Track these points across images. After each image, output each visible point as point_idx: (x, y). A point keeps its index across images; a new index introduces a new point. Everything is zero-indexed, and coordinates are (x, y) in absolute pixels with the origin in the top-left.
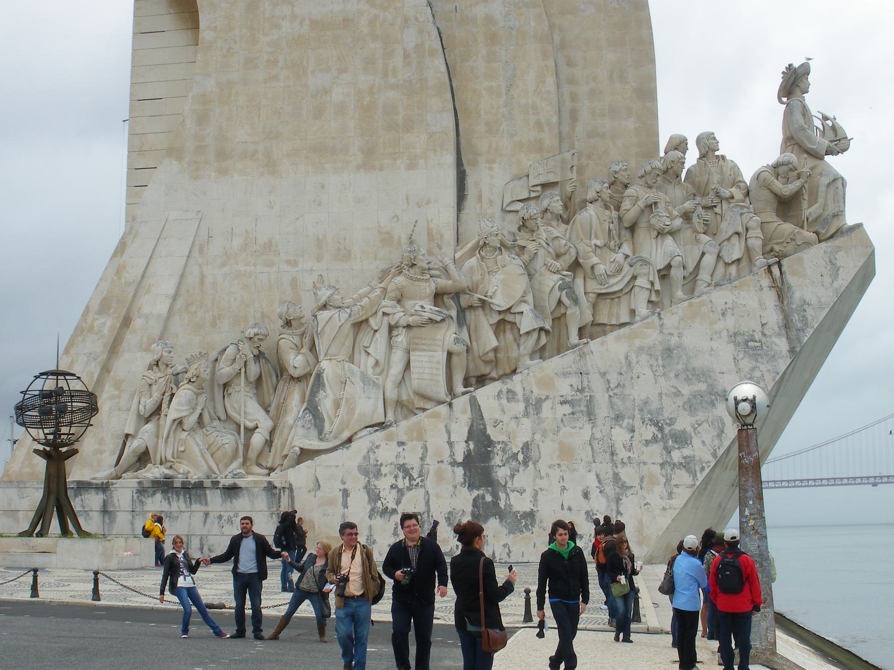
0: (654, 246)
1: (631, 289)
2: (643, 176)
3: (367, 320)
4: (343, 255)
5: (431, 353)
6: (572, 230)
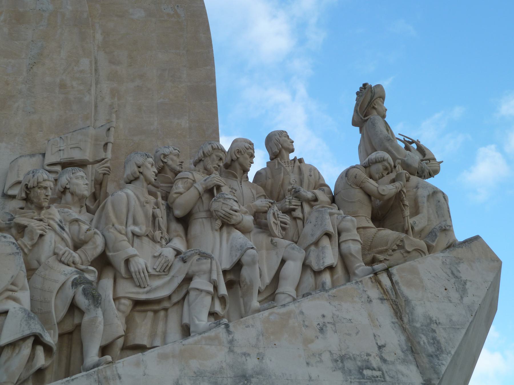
1: (184, 298)
2: (200, 160)
6: (100, 217)
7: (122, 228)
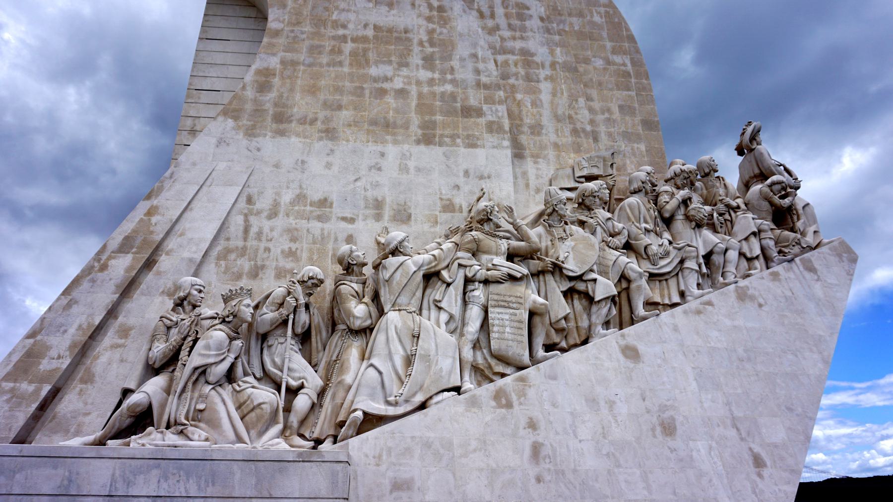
0: (694, 236)
2: (672, 178)
3: (437, 274)
4: (403, 216)
5: (512, 311)
7: (638, 225)
